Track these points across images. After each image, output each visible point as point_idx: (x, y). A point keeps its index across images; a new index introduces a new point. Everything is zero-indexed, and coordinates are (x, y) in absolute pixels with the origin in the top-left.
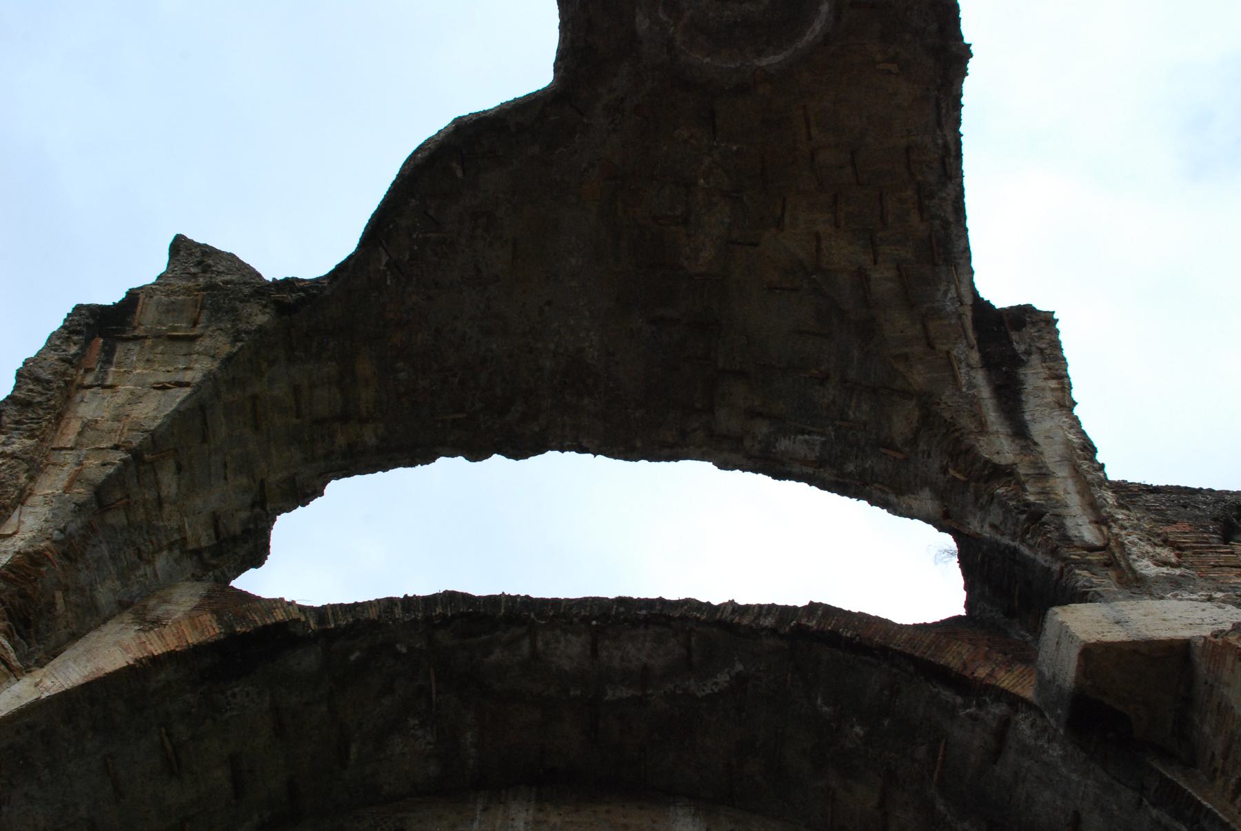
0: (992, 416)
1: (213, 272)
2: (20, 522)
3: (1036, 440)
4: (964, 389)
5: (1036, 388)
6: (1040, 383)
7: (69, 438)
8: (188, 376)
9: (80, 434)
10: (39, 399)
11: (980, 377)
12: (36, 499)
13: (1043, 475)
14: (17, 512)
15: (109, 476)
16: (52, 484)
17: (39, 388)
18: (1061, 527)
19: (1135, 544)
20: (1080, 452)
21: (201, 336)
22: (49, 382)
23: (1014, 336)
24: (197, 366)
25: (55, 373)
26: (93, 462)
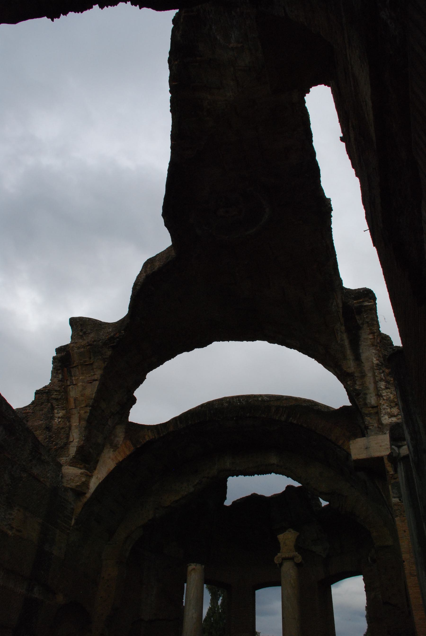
0: (349, 352)
1: (87, 334)
2: (73, 436)
3: (363, 361)
4: (339, 342)
5: (364, 339)
6: (366, 337)
7: (72, 405)
8: (96, 377)
9: (75, 403)
10: (59, 397)
11: (345, 336)
12: (73, 428)
13: (363, 376)
14: (71, 433)
15: (89, 416)
16: (75, 422)
17: (58, 393)
18: (365, 399)
19: (384, 409)
20: (376, 368)
21: (94, 362)
22: (59, 390)
23: (357, 317)
24: (97, 373)
25: (59, 387)
26: (82, 412)
